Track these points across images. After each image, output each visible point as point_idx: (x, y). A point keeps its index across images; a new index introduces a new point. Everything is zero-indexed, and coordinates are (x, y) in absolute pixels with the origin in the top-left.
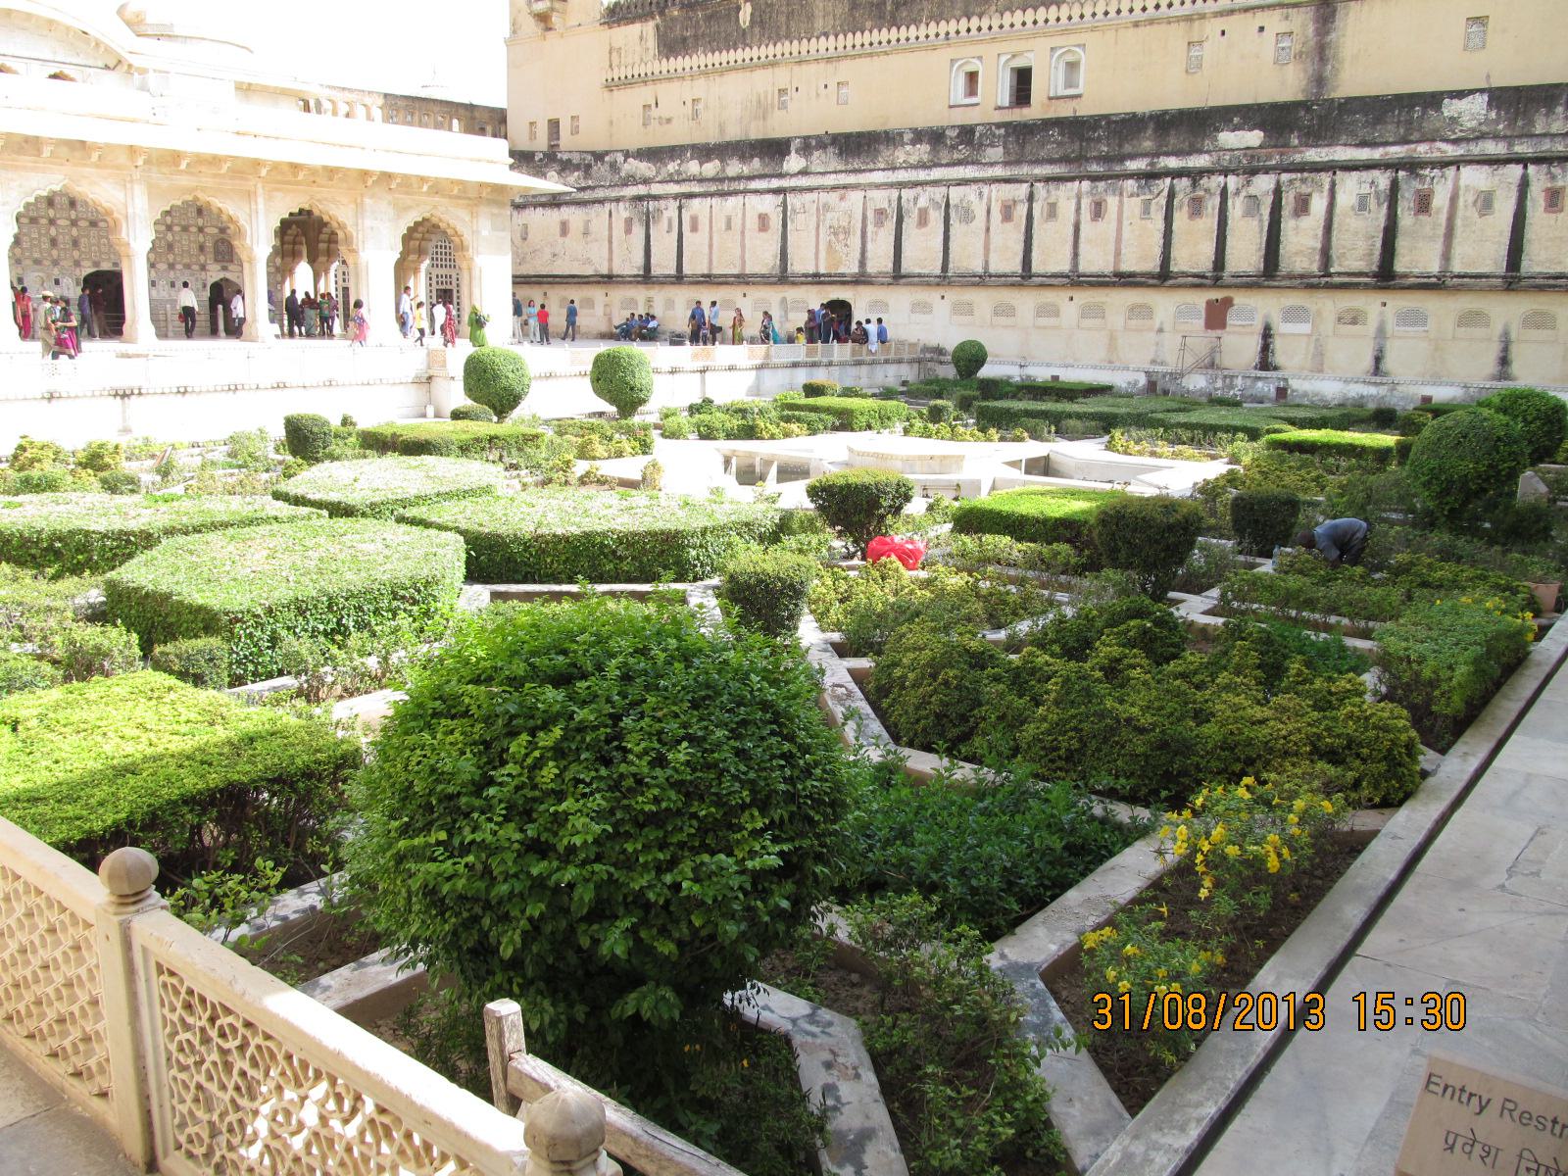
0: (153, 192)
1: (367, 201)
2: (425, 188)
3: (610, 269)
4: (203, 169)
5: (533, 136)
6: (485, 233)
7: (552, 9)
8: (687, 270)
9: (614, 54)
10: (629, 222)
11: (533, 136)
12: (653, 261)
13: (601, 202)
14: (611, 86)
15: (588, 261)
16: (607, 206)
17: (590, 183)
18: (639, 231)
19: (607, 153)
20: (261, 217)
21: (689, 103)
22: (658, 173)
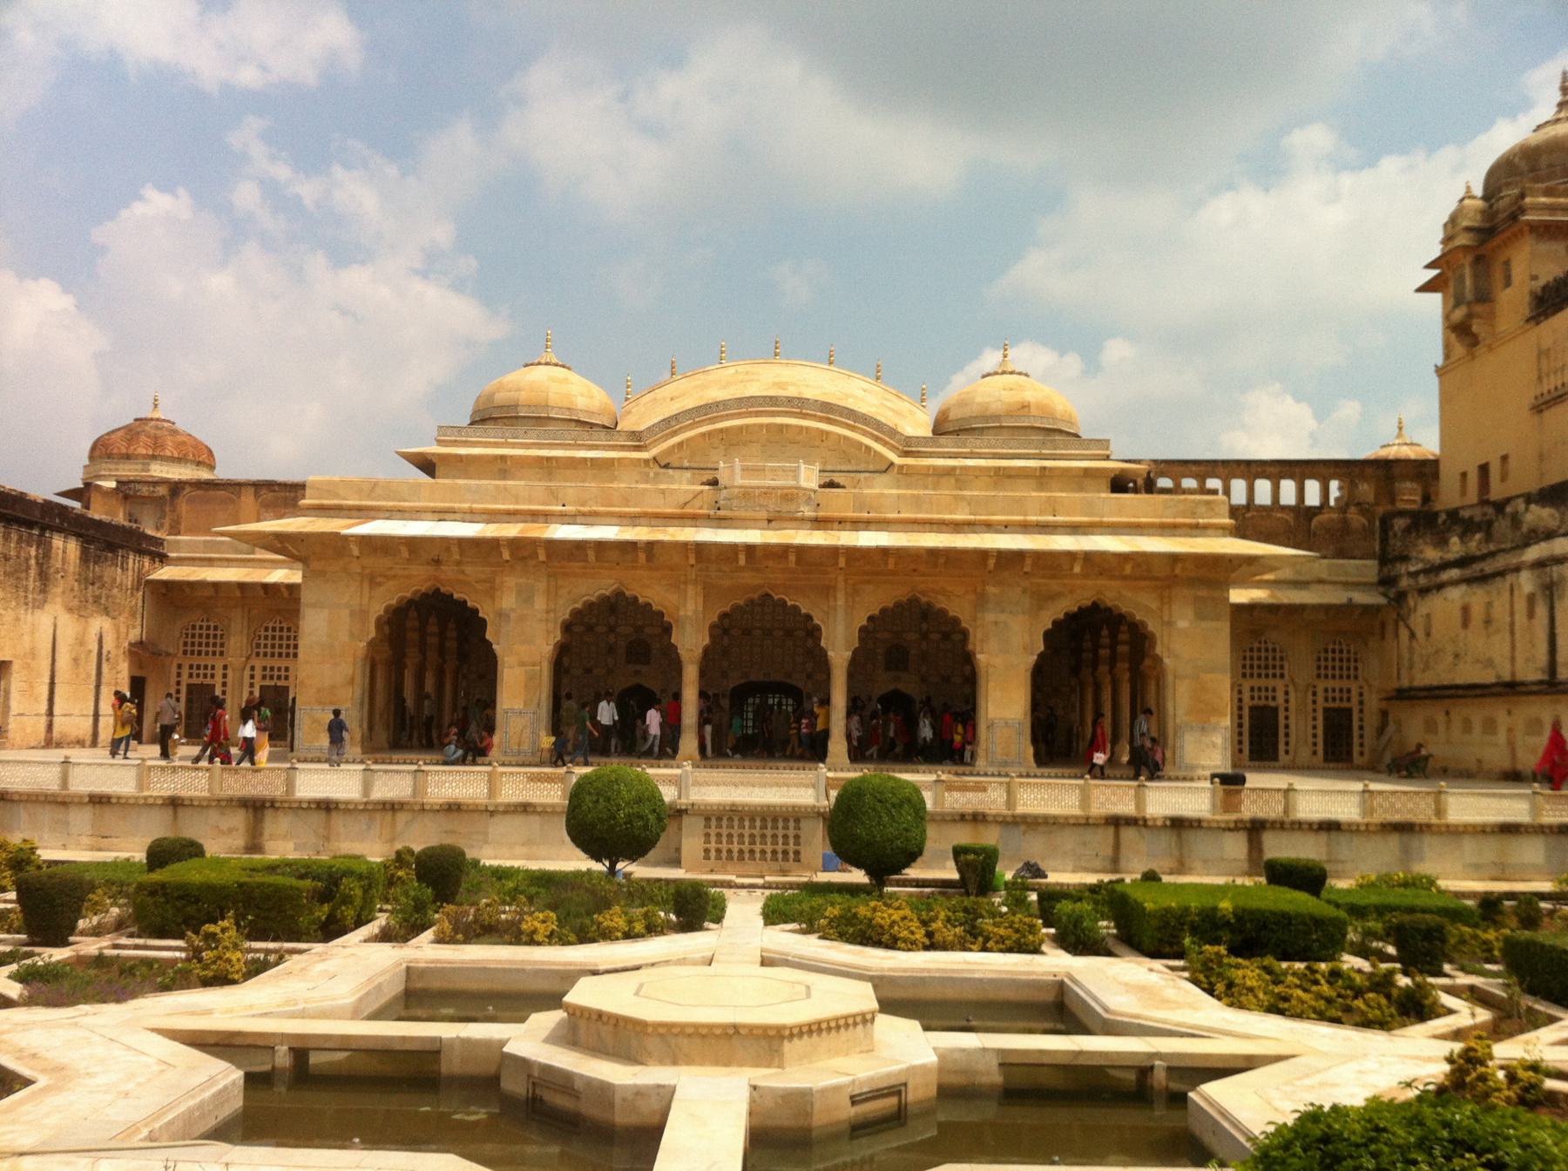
0: (709, 592)
1: (992, 590)
2: (1077, 569)
3: (1513, 674)
4: (771, 564)
5: (1463, 492)
6: (1183, 624)
7: (1470, 316)
9: (1544, 361)
10: (1531, 599)
11: (1463, 492)
12: (1560, 658)
13: (1501, 574)
14: (1541, 406)
15: (1489, 663)
16: (1510, 578)
17: (1492, 547)
18: (1541, 611)
19: (1508, 500)
20: (840, 615)
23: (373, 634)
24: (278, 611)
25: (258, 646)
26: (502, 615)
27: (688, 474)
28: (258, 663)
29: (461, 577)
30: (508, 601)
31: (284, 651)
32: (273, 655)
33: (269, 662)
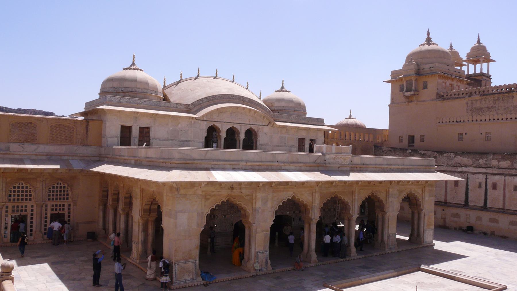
1: (391, 190)
5: (401, 141)
6: (427, 199)
8: (489, 205)
11: (401, 141)
12: (470, 199)
21: (484, 134)
22: (474, 163)
23: (205, 223)
24: (23, 179)
25: (10, 196)
26: (255, 210)
27: (205, 123)
28: (10, 205)
29: (240, 194)
30: (258, 204)
31: (24, 198)
32: (18, 200)
33: (16, 204)
